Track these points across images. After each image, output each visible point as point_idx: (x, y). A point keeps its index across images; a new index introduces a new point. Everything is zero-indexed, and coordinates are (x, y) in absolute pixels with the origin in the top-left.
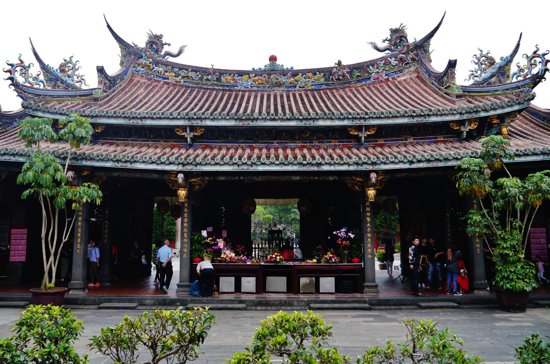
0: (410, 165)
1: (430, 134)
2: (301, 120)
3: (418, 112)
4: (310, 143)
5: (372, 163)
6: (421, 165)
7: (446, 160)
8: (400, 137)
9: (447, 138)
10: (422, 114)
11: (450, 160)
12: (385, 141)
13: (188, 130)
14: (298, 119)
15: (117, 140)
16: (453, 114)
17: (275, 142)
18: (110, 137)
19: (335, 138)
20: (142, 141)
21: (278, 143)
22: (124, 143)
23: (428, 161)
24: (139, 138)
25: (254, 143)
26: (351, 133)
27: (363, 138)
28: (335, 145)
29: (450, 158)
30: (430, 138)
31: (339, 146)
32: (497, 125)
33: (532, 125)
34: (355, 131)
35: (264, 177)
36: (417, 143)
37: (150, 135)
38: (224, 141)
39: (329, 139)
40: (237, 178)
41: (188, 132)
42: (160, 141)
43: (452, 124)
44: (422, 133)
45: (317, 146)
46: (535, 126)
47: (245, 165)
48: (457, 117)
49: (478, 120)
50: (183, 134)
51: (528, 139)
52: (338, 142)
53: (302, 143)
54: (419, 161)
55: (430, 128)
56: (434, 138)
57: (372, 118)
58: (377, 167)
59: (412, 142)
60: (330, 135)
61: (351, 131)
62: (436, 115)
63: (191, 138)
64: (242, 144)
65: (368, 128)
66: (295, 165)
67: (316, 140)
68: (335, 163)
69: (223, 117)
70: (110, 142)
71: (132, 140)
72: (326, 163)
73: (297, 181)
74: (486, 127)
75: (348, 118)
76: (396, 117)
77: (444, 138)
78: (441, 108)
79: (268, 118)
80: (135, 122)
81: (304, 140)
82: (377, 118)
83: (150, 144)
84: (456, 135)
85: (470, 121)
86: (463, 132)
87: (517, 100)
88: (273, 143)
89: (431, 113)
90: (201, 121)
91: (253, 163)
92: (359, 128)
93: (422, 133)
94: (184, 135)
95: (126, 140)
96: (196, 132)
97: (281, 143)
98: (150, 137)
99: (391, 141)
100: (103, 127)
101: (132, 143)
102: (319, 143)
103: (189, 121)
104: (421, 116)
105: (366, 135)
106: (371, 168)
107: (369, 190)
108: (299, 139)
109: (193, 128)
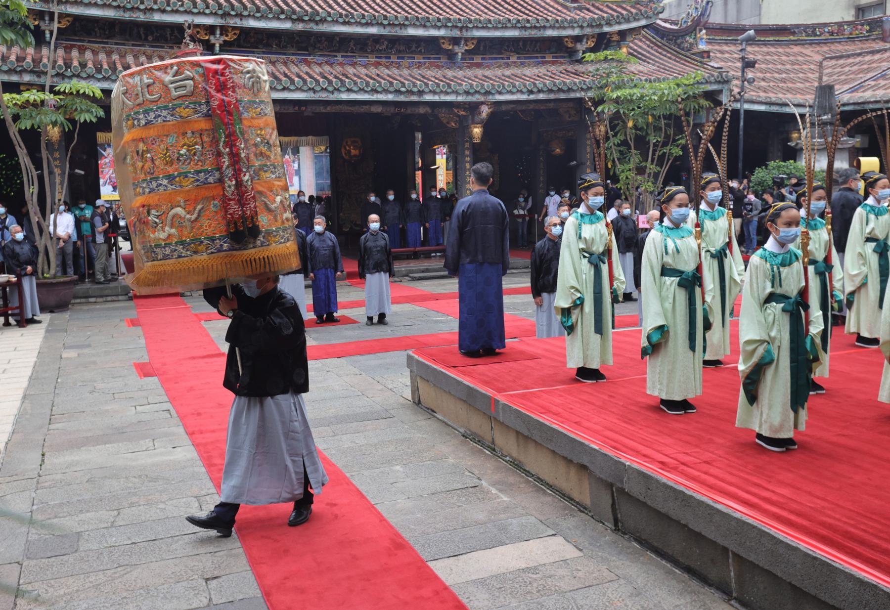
0: (529, 95)
1: (537, 52)
2: (384, 26)
3: (534, 22)
4: (386, 58)
5: (485, 93)
6: (541, 96)
7: (570, 90)
8: (501, 53)
9: (556, 57)
10: (538, 25)
11: (574, 91)
12: (483, 59)
13: (218, 32)
14: (381, 24)
15: (89, 42)
16: (573, 27)
17: (339, 55)
18: (76, 35)
19: (420, 53)
20: (133, 45)
21: (342, 57)
22: (103, 47)
23: (550, 91)
24: (128, 40)
25: (309, 55)
26: (443, 46)
27: (460, 54)
28: (419, 63)
29: (575, 88)
30: (537, 58)
31: (425, 64)
32: (615, 43)
33: (647, 42)
34: (450, 45)
35: (334, 108)
36: (522, 64)
37: (146, 36)
38: (264, 50)
39: (412, 52)
40: (297, 108)
41: (218, 36)
42: (163, 47)
43: (567, 39)
44: (528, 50)
45: (396, 64)
46: (652, 45)
47: (324, 91)
48: (577, 32)
49: (596, 36)
50: (207, 38)
51: (649, 63)
52: (424, 58)
53: (377, 57)
54: (540, 91)
55: (539, 44)
56: (542, 57)
57: (477, 27)
58: (491, 98)
59: (515, 62)
60: (414, 48)
61: (443, 43)
62: (552, 27)
63: (220, 45)
64: (291, 57)
65: (467, 40)
66: (391, 92)
67: (395, 54)
68: (442, 92)
69: (252, 14)
70: (79, 46)
71: (116, 44)
72: (430, 91)
73: (378, 114)
74: (604, 46)
75: (446, 26)
76: (506, 27)
77: (553, 57)
78: (559, 18)
79: (341, 20)
80: (135, 16)
81: (379, 54)
82: (483, 28)
83: (149, 52)
84: (567, 55)
85: (588, 37)
86: (578, 51)
87: (646, 12)
88: (336, 56)
89: (548, 25)
90: (241, 20)
91: (335, 89)
92: (455, 41)
93: (528, 50)
94: (208, 40)
95: (107, 43)
96: (227, 36)
97: (347, 56)
98: (146, 39)
99: (491, 59)
100: (70, 19)
101: (117, 49)
102: (398, 58)
103: (222, 18)
104: (535, 27)
105: (463, 51)
106: (482, 98)
107: (476, 127)
108: (372, 51)
109: (224, 29)
